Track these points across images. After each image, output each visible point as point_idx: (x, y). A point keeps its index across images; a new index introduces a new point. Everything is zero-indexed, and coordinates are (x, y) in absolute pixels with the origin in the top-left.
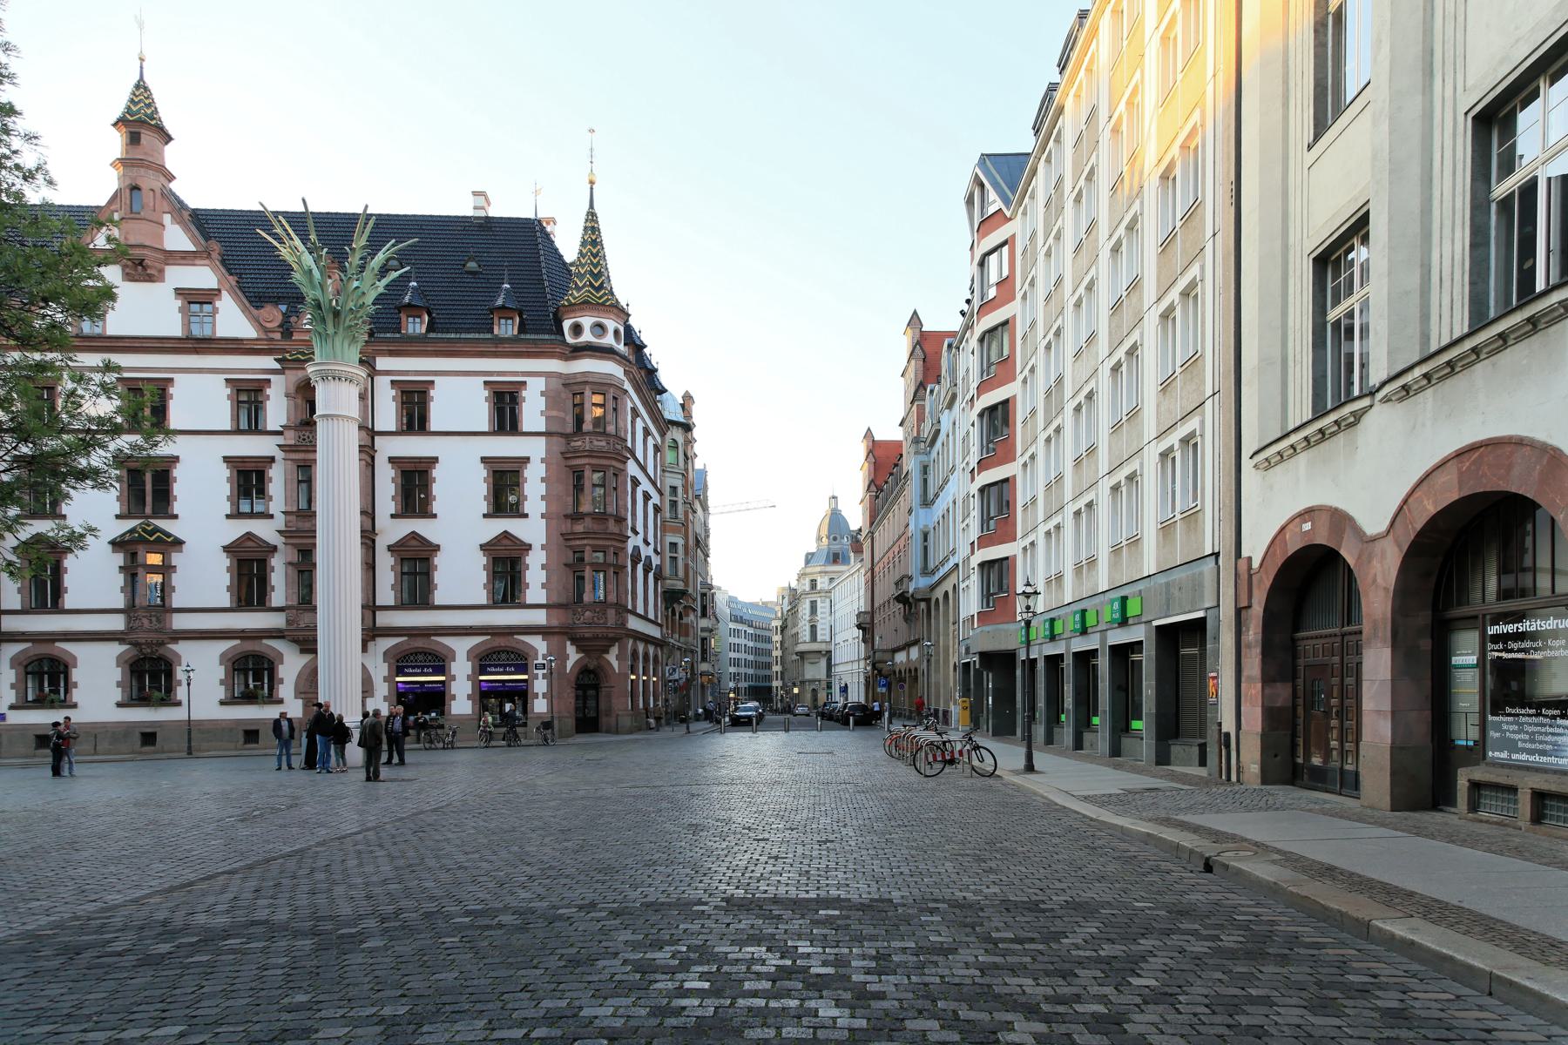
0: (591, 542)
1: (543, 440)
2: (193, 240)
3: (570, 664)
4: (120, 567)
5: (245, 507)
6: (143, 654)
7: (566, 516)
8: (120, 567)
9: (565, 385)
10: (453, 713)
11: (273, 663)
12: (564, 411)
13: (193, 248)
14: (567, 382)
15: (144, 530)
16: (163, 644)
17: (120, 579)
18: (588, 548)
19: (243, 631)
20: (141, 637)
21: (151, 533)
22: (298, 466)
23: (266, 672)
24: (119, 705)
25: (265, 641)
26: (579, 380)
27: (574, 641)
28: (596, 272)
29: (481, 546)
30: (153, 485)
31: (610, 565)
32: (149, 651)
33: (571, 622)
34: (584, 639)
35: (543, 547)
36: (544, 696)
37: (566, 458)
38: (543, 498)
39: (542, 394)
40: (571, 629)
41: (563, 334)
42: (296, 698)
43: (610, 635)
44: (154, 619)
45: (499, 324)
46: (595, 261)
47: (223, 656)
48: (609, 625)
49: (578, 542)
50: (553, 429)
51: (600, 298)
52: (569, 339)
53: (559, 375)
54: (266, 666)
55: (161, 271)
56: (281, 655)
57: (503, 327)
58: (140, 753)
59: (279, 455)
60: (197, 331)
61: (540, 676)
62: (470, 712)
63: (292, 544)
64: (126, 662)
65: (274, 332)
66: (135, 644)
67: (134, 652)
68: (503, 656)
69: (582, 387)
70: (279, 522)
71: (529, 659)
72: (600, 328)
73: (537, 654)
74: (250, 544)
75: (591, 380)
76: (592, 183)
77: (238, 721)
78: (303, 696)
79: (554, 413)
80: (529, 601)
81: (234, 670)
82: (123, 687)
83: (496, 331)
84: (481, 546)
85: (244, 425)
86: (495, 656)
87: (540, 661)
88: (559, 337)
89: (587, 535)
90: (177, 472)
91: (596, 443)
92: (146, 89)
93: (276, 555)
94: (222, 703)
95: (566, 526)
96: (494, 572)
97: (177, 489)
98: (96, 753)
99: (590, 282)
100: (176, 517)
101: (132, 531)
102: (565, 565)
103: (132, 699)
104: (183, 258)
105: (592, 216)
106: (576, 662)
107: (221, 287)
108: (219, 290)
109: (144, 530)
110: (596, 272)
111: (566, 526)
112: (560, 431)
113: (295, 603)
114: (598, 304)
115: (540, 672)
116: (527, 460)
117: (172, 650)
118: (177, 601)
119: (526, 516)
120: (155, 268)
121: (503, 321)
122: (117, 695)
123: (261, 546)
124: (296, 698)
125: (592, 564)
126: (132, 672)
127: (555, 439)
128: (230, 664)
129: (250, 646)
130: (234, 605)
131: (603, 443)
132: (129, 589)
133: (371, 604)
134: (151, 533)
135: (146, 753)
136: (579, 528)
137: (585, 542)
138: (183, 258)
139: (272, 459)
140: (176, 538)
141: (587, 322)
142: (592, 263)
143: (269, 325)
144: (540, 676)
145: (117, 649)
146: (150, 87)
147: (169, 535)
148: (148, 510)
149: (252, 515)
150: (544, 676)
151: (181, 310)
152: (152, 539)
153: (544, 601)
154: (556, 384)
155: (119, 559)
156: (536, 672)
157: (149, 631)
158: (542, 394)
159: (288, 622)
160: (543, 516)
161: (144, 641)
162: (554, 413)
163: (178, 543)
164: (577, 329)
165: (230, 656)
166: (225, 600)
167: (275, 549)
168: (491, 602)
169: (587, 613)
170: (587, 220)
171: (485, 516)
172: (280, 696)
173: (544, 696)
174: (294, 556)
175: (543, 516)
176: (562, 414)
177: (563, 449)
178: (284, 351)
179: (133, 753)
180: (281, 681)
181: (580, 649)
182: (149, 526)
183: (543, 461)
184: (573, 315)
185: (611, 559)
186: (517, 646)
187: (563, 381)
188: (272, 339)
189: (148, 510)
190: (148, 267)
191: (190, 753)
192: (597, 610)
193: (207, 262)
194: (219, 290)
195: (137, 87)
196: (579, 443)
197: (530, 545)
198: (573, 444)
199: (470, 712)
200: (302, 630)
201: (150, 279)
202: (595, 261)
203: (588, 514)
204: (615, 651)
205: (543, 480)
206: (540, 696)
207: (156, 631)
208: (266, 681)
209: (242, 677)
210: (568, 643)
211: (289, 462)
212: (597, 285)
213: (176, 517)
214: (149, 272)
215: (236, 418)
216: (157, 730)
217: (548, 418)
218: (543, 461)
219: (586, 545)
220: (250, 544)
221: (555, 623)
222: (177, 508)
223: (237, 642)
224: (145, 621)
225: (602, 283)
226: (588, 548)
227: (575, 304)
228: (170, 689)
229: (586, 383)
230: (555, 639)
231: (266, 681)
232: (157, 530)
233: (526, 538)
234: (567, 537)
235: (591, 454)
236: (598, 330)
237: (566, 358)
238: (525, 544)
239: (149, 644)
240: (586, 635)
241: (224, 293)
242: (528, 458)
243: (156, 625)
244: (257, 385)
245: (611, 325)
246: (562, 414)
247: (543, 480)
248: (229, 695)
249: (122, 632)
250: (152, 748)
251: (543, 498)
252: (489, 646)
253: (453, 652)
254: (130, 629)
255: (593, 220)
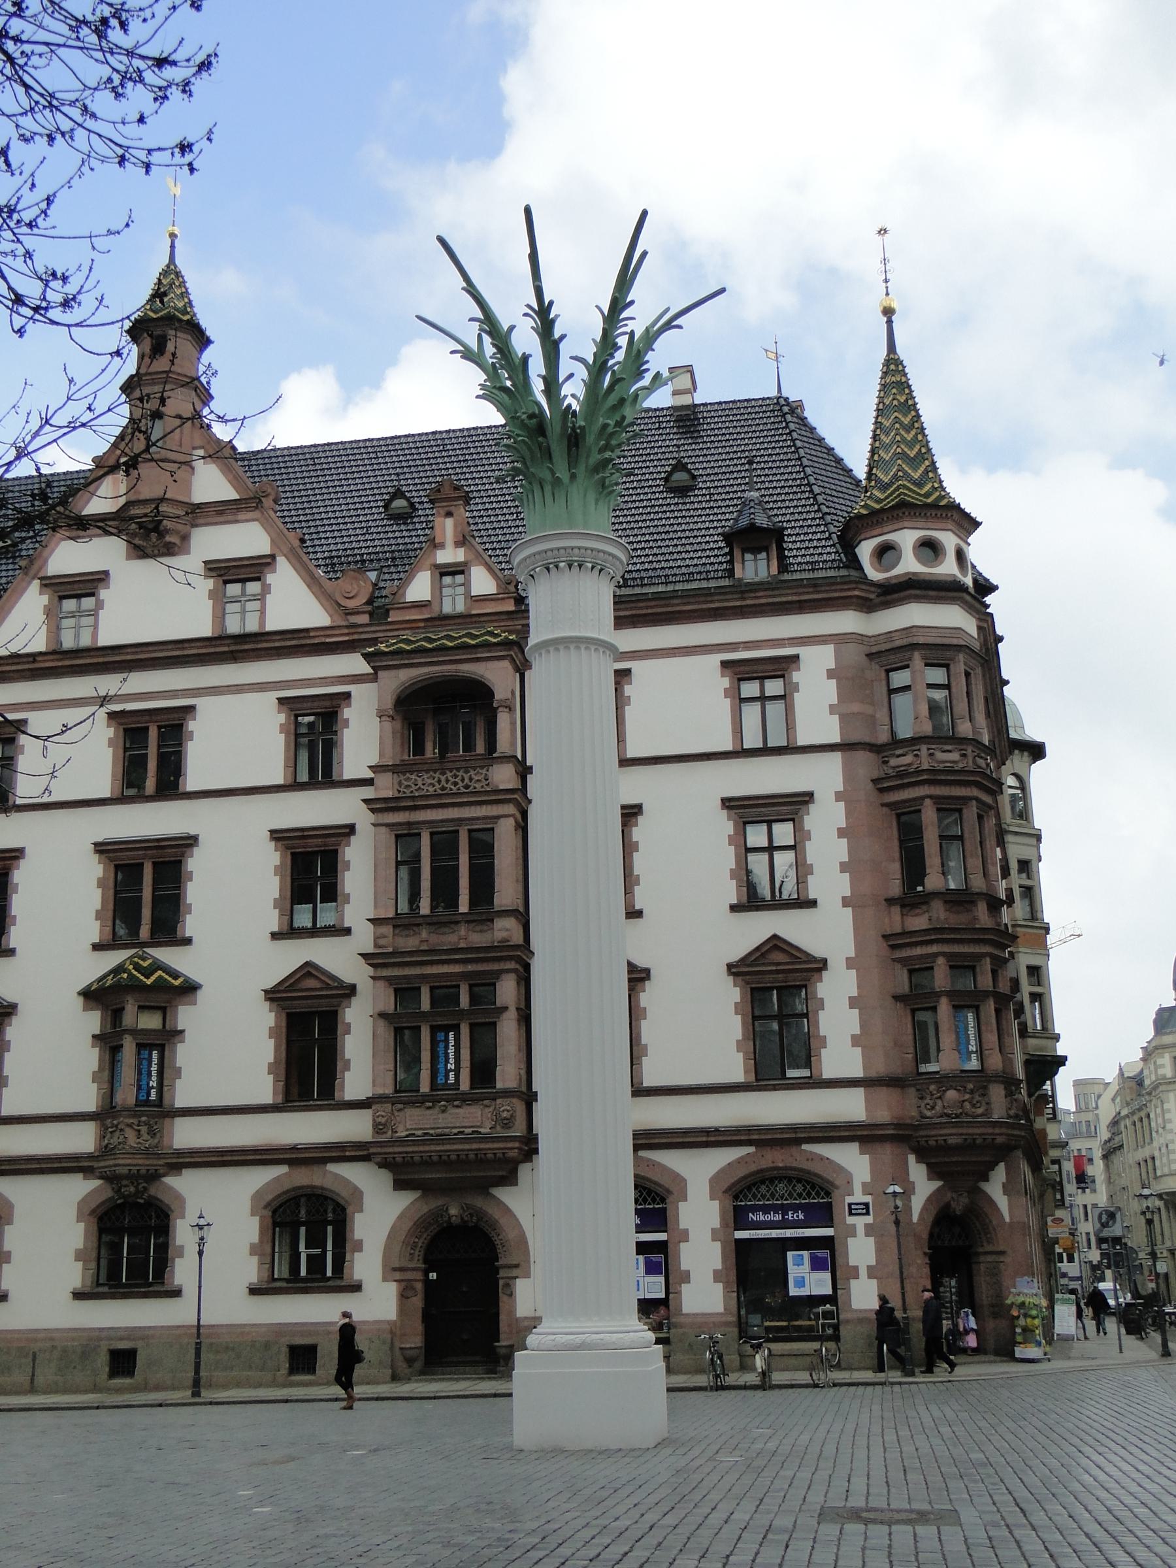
0: (946, 948)
1: (836, 757)
2: (235, 481)
3: (918, 1203)
4: (94, 1036)
5: (303, 917)
6: (124, 1197)
7: (890, 901)
8: (94, 1036)
9: (870, 656)
10: (685, 1310)
11: (344, 1210)
12: (872, 704)
13: (234, 495)
14: (875, 649)
15: (137, 967)
16: (154, 1177)
17: (91, 1058)
18: (941, 961)
19: (294, 1148)
20: (123, 1164)
21: (147, 973)
22: (397, 836)
23: (330, 1229)
24: (78, 1295)
25: (332, 1167)
26: (898, 643)
27: (923, 1154)
28: (912, 454)
29: (730, 966)
30: (154, 890)
31: (986, 994)
32: (132, 1189)
33: (914, 1113)
34: (946, 1149)
35: (850, 963)
36: (872, 1273)
37: (881, 790)
38: (844, 867)
39: (831, 674)
40: (917, 1128)
41: (860, 568)
42: (385, 1279)
43: (1000, 1140)
44: (144, 1129)
45: (743, 561)
46: (909, 437)
47: (257, 1196)
48: (995, 1117)
49: (919, 951)
50: (855, 737)
51: (927, 495)
52: (873, 574)
53: (860, 638)
54: (330, 1216)
55: (185, 538)
56: (358, 1194)
57: (750, 565)
58: (109, 1390)
59: (363, 819)
60: (233, 627)
61: (861, 1230)
62: (721, 1309)
63: (388, 979)
64: (93, 1212)
65: (358, 613)
66: (110, 1178)
67: (108, 1193)
68: (781, 1188)
69: (907, 655)
70: (364, 938)
71: (836, 1194)
72: (930, 548)
73: (849, 1182)
74: (311, 983)
75: (921, 640)
76: (888, 312)
77: (280, 1329)
78: (398, 1275)
79: (856, 707)
80: (828, 1073)
81: (275, 1224)
82: (85, 1261)
83: (738, 573)
84: (730, 966)
85: (304, 777)
86: (763, 1189)
87: (858, 1197)
88: (853, 573)
89: (935, 934)
90: (195, 863)
91: (940, 756)
92: (178, 274)
93: (354, 1001)
94: (254, 1291)
95: (895, 921)
96: (754, 1018)
97: (193, 893)
98: (32, 1389)
99: (905, 473)
100: (188, 941)
101: (117, 970)
102: (896, 998)
103: (98, 1285)
104: (222, 512)
105: (893, 368)
106: (929, 1200)
107: (276, 552)
108: (273, 557)
109: (137, 967)
110: (912, 454)
111: (895, 921)
112: (867, 739)
113: (389, 1090)
114: (926, 505)
115: (860, 1222)
116: (807, 798)
117: (171, 1188)
118: (183, 1095)
119: (813, 904)
120: (177, 532)
121: (748, 556)
122: (75, 1275)
123: (328, 987)
124: (385, 1279)
125: (950, 994)
126: (101, 1231)
127: (861, 756)
128: (268, 1213)
129: (304, 1177)
130: (280, 1099)
131: (955, 756)
132: (106, 1073)
133: (524, 1089)
134: (147, 973)
135: (119, 1390)
136: (919, 922)
137: (934, 949)
138: (221, 513)
139: (350, 829)
140: (187, 980)
141: (907, 538)
142: (904, 440)
143: (351, 604)
144: (861, 1230)
145: (79, 1188)
146: (183, 273)
147: (175, 975)
148: (145, 932)
149: (314, 932)
150: (869, 1230)
151: (212, 594)
152: (149, 982)
153: (857, 1072)
154: (855, 654)
155: (93, 1021)
156: (850, 1220)
157: (136, 1152)
158: (831, 674)
159: (378, 1128)
160: (846, 902)
161: (124, 1171)
162: (856, 707)
163: (190, 989)
164: (885, 551)
165: (270, 1197)
166: (264, 1090)
167: (351, 990)
168: (752, 1078)
169: (951, 1094)
170: (885, 374)
171: (734, 908)
172: (357, 1277)
173: (872, 1273)
174: (388, 1003)
175: (846, 902)
176: (869, 710)
177: (875, 775)
178: (374, 641)
179: (95, 1389)
180: (359, 1246)
181: (934, 1172)
182: (144, 959)
183: (839, 796)
184: (875, 532)
185: (985, 981)
186: (805, 1165)
187: (868, 650)
188: (355, 626)
189: (145, 932)
190: (167, 531)
191: (197, 1386)
192: (970, 1086)
193: (256, 514)
194: (273, 557)
195: (165, 273)
196: (908, 759)
197: (825, 961)
198: (893, 762)
199: (721, 1309)
200: (402, 1142)
201: (170, 550)
202: (909, 437)
203: (935, 894)
204: (999, 1174)
205: (841, 833)
206: (863, 1272)
207: (148, 1153)
208: (329, 1247)
209: (287, 1239)
210: (912, 1158)
211: (383, 829)
212: (916, 475)
213: (188, 941)
214: (168, 538)
215: (293, 764)
216: (139, 1345)
217: (845, 720)
218: (839, 796)
219: (936, 955)
220: (311, 983)
221: (883, 1116)
222: (191, 925)
223: (283, 1169)
224: (130, 1134)
225: (926, 472)
226: (941, 961)
227: (882, 510)
228: (163, 1264)
229: (914, 646)
230: (887, 1151)
231: (329, 1247)
232: (158, 966)
233: (817, 950)
234: (894, 941)
235: (935, 777)
236: (928, 552)
237: (867, 606)
238: (814, 960)
239: (133, 1177)
240: (952, 1141)
241: (282, 561)
242: (810, 795)
243: (147, 1141)
244: (328, 704)
245: (948, 540)
246: (869, 710)
247: (841, 833)
248: (266, 1275)
249: (90, 1157)
250: (127, 1381)
251: (844, 867)
252: (753, 1168)
253: (681, 1181)
254: (105, 1151)
255: (897, 371)
